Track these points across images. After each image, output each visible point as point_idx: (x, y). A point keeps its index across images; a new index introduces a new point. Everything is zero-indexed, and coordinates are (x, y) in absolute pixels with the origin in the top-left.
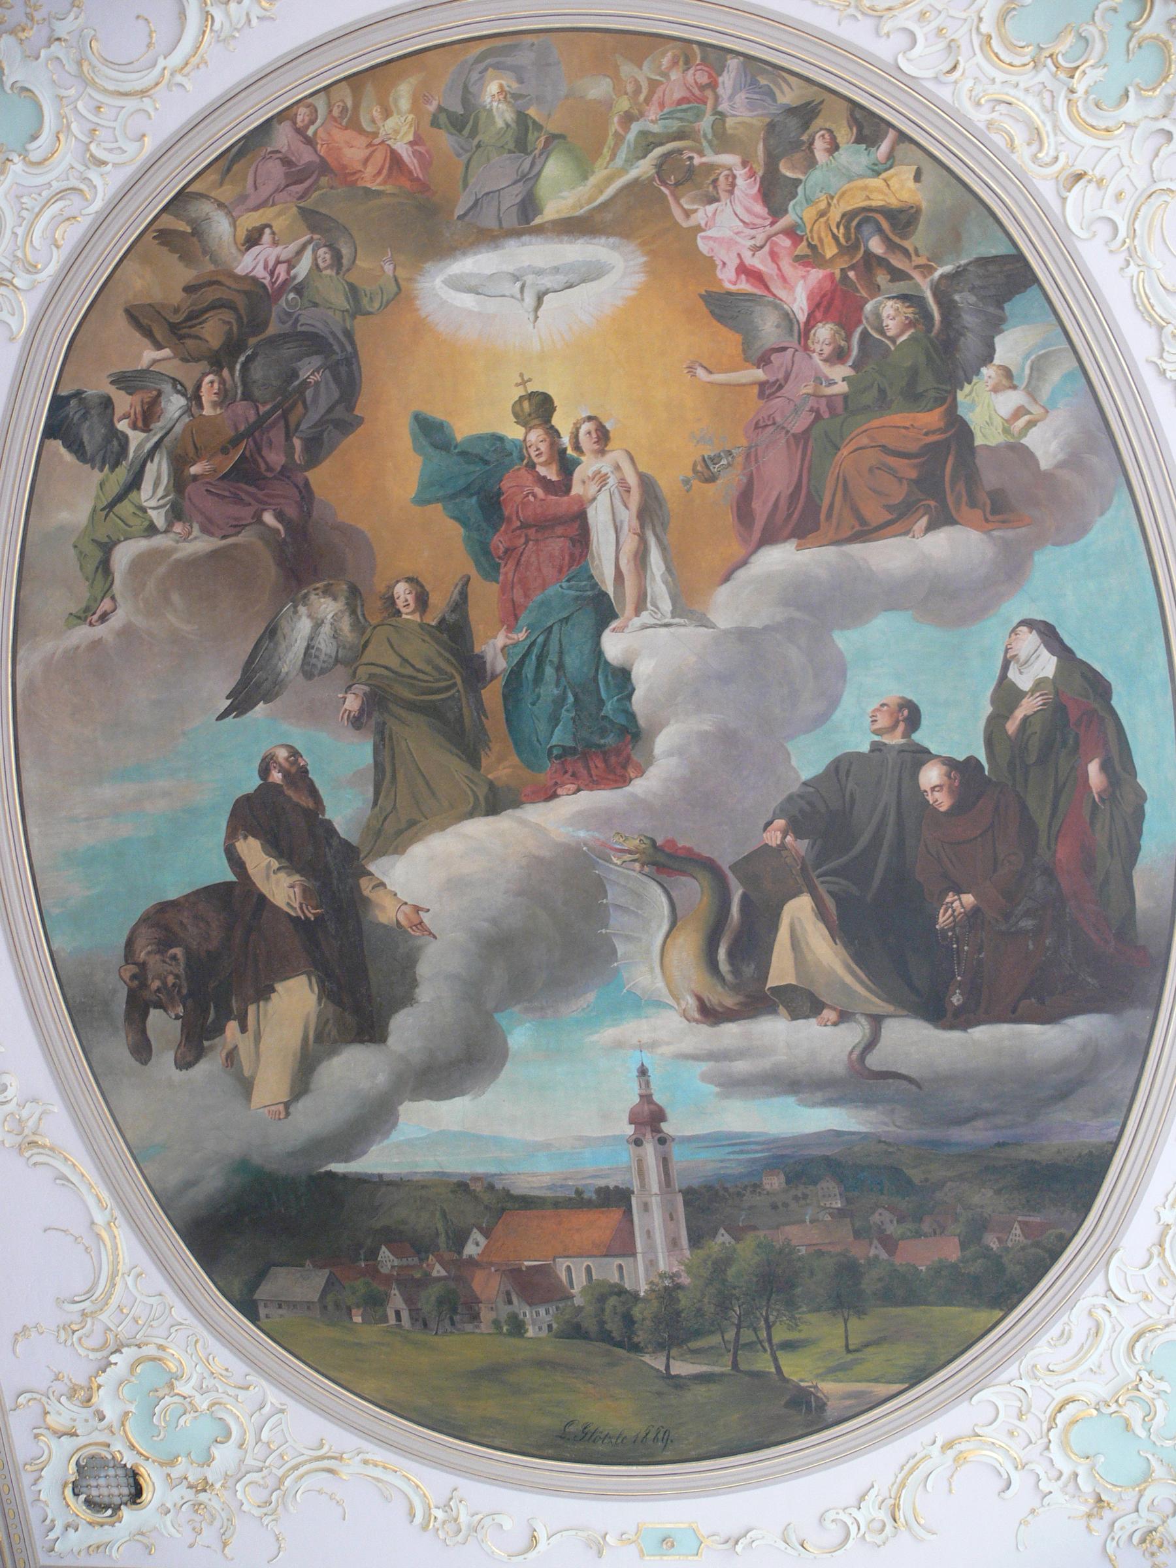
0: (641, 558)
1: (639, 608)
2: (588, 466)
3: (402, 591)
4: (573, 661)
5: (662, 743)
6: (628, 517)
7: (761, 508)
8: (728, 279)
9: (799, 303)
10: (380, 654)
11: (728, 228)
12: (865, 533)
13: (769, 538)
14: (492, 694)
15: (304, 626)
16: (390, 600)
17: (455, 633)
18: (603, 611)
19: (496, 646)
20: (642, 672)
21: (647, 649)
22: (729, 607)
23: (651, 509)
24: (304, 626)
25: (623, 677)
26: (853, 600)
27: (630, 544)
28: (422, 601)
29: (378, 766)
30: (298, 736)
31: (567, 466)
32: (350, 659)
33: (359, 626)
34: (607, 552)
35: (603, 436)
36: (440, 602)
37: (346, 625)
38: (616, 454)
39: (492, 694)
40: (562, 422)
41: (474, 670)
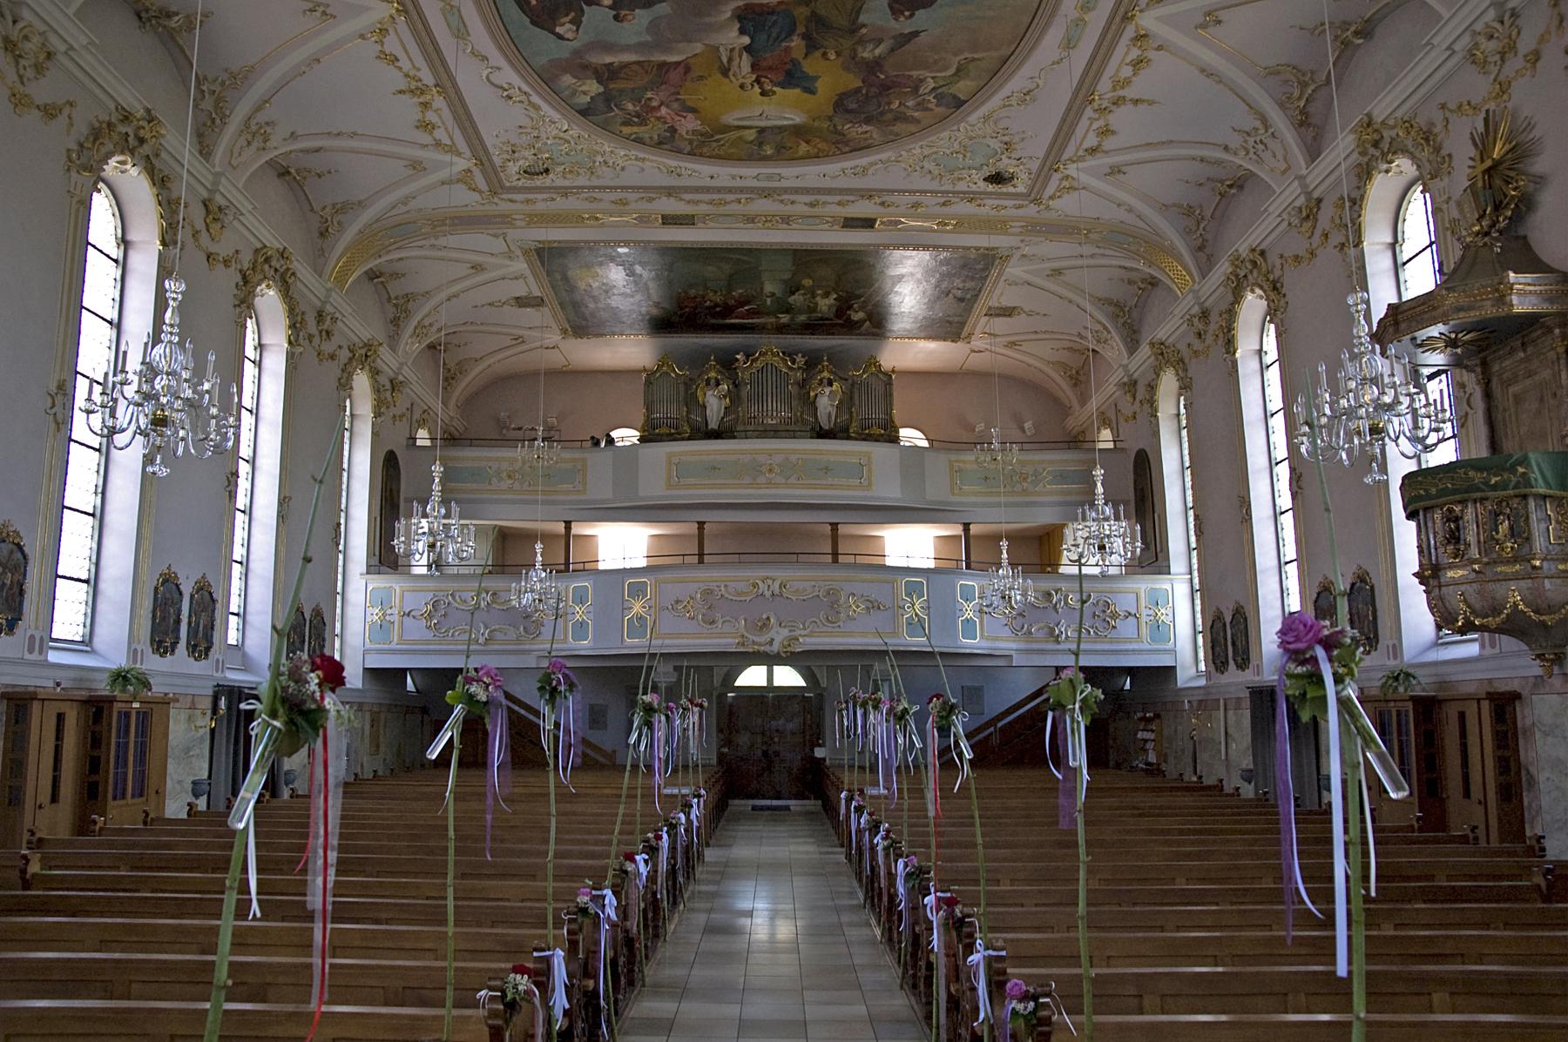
0: (730, 60)
1: (732, 50)
2: (748, 81)
3: (833, 57)
4: (764, 37)
5: (729, 14)
6: (734, 68)
7: (681, 69)
8: (690, 116)
9: (664, 110)
10: (847, 43)
11: (688, 125)
12: (638, 63)
13: (678, 63)
14: (801, 29)
15: (877, 52)
16: (838, 54)
17: (812, 46)
18: (747, 49)
19: (796, 43)
20: (734, 33)
21: (733, 38)
22: (698, 48)
23: (725, 72)
24: (877, 52)
25: (742, 32)
26: (641, 47)
27: (735, 63)
28: (824, 55)
29: (858, 13)
30: (893, 24)
31: (758, 81)
32: (862, 42)
33: (855, 50)
34: (746, 61)
35: (742, 86)
36: (818, 54)
37: (860, 49)
38: (737, 83)
39: (801, 29)
40: (757, 89)
41: (806, 36)
